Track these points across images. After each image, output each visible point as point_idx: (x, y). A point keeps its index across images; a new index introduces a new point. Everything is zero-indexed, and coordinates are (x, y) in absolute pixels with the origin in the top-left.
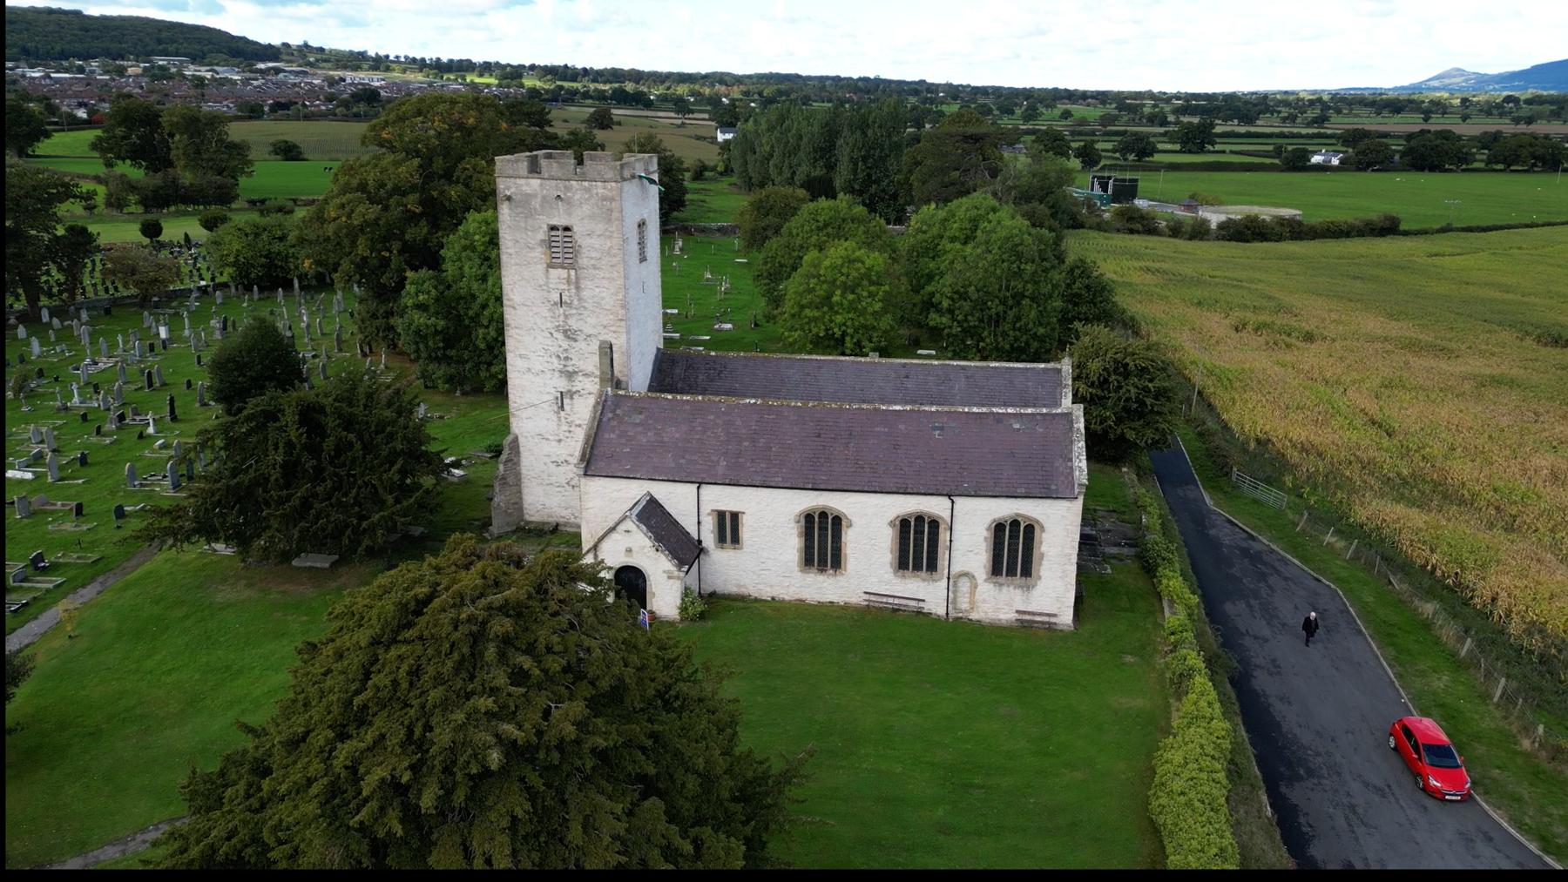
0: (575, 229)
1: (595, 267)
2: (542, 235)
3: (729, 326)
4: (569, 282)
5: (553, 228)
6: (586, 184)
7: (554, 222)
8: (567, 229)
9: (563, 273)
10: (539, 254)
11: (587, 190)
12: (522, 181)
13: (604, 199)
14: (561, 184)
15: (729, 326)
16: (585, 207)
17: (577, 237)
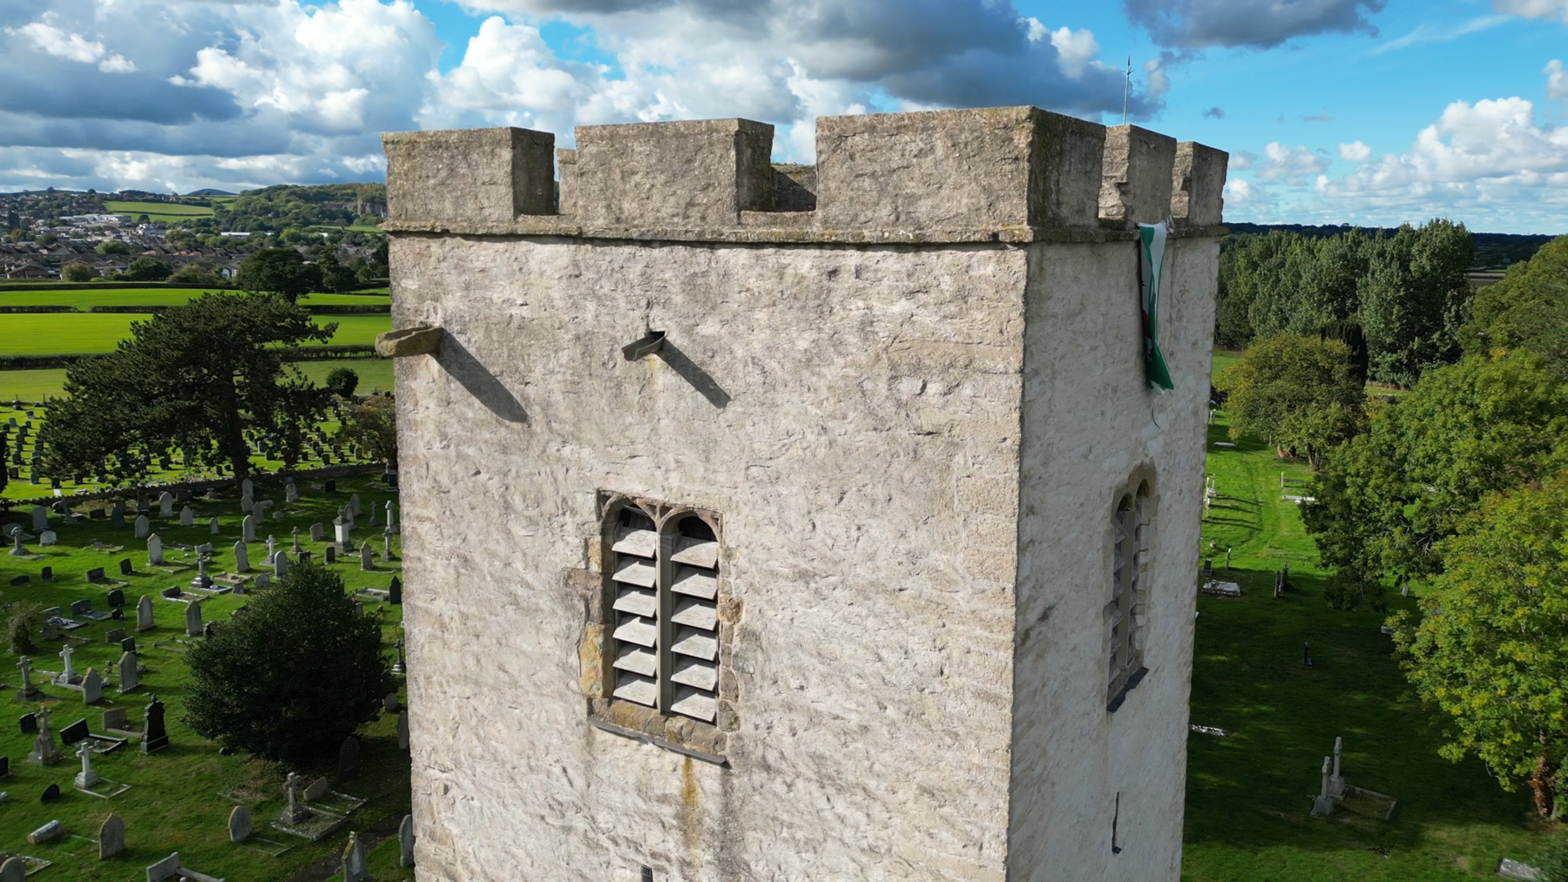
0: (733, 529)
1: (827, 779)
2: (570, 544)
3: (1232, 587)
4: (687, 823)
5: (623, 515)
6: (804, 262)
7: (634, 484)
8: (692, 526)
9: (664, 765)
10: (553, 648)
11: (815, 302)
12: (485, 254)
13: (903, 360)
14: (668, 264)
15: (1232, 587)
16: (794, 410)
17: (732, 583)
